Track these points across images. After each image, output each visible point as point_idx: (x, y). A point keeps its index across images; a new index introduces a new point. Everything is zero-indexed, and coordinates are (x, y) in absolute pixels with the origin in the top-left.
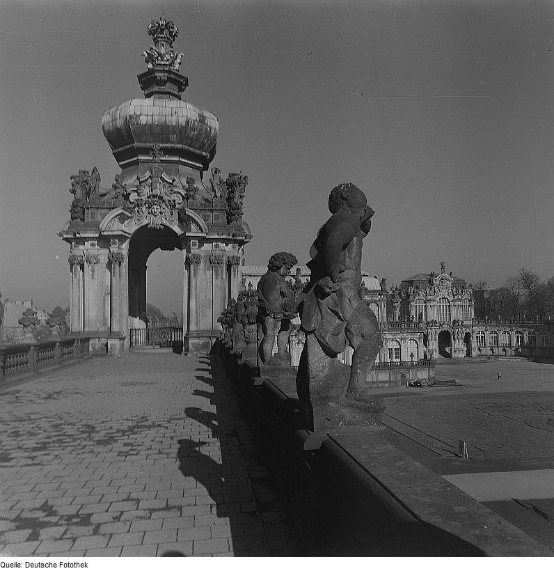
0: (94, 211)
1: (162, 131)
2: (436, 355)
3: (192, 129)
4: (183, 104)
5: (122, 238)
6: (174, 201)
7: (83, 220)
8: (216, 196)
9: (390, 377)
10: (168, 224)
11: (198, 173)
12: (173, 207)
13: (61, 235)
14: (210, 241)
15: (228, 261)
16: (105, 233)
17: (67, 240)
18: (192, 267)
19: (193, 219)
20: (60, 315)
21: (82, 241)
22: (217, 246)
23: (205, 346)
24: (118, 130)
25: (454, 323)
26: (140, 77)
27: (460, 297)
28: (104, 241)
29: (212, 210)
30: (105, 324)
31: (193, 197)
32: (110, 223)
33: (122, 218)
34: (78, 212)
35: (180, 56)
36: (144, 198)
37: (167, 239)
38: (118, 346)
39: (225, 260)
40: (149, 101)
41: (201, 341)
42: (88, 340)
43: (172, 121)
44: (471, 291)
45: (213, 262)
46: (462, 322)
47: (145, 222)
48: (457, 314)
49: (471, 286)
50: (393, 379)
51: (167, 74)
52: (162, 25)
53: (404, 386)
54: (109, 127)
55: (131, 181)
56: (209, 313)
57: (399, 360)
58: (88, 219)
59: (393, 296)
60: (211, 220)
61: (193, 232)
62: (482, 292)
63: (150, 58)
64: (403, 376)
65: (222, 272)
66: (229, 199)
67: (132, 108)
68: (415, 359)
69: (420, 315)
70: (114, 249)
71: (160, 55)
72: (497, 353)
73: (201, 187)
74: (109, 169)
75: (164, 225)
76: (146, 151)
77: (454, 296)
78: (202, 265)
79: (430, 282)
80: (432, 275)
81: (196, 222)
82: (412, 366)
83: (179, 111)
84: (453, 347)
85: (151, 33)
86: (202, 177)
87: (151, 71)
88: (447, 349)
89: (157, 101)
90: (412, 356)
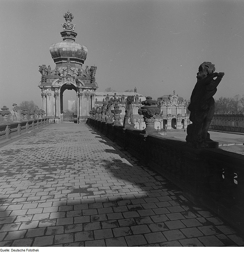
0: (49, 79)
1: (70, 53)
3: (79, 52)
5: (58, 88)
7: (46, 82)
8: (87, 74)
12: (74, 78)
14: (85, 89)
16: (54, 87)
17: (41, 88)
18: (80, 97)
21: (46, 88)
23: (84, 121)
25: (178, 115)
26: (61, 33)
27: (181, 105)
28: (53, 89)
30: (53, 114)
32: (55, 83)
33: (58, 82)
34: (44, 80)
35: (74, 25)
36: (65, 75)
37: (71, 87)
39: (90, 95)
41: (83, 119)
43: (73, 50)
45: (86, 95)
46: (181, 115)
48: (179, 111)
55: (60, 69)
56: (85, 111)
60: (86, 82)
61: (81, 86)
63: (64, 26)
66: (91, 75)
67: (60, 45)
68: (160, 128)
70: (56, 91)
78: (83, 96)
84: (177, 125)
85: (65, 17)
88: (175, 126)
90: (158, 127)
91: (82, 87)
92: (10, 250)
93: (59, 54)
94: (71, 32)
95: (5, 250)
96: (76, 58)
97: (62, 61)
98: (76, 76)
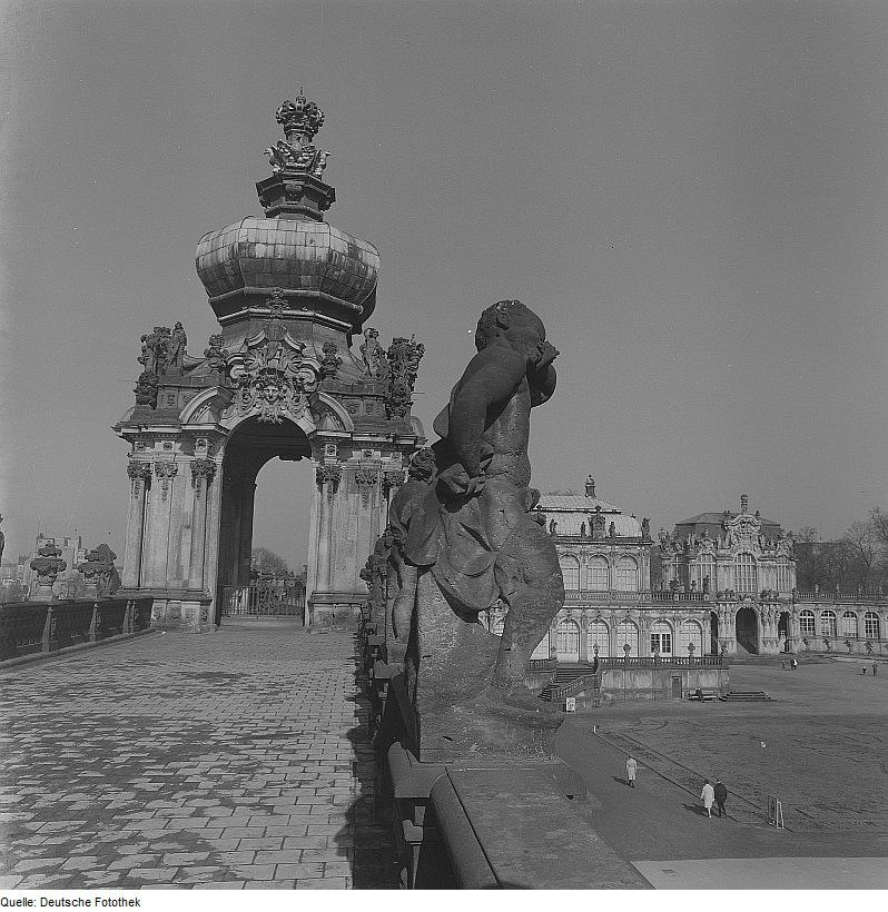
0: (172, 392)
1: (288, 270)
2: (733, 649)
3: (338, 267)
4: (323, 227)
6: (302, 379)
7: (154, 406)
9: (654, 683)
10: (290, 416)
11: (343, 337)
12: (299, 388)
13: (117, 429)
14: (358, 446)
15: (385, 479)
16: (187, 428)
17: (126, 436)
19: (331, 409)
20: (102, 561)
21: (152, 439)
22: (368, 455)
23: (341, 619)
24: (220, 267)
28: (188, 439)
29: (361, 396)
31: (333, 373)
34: (148, 391)
36: (253, 373)
37: (293, 444)
38: (198, 613)
39: (380, 476)
40: (272, 223)
41: (336, 610)
42: (150, 600)
43: (306, 253)
44: (791, 544)
47: (255, 411)
49: (790, 535)
50: (659, 685)
51: (302, 183)
52: (299, 108)
53: (677, 700)
54: (207, 261)
55: (235, 347)
57: (670, 655)
58: (162, 405)
59: (662, 548)
60: (361, 411)
62: (809, 545)
63: (278, 157)
64: (677, 681)
65: (374, 496)
67: (243, 232)
69: (706, 580)
71: (293, 153)
72: (834, 649)
73: (346, 359)
74: (201, 326)
75: (282, 417)
76: (261, 300)
77: (763, 550)
79: (723, 526)
80: (726, 514)
81: (335, 413)
82: (692, 665)
83: (316, 239)
86: (350, 344)
87: (278, 177)
89: (283, 222)
91: (339, 434)
92: (37, 903)
93: (238, 274)
94: (306, 179)
95: (19, 901)
96: (317, 293)
97: (251, 310)
98: (309, 377)
